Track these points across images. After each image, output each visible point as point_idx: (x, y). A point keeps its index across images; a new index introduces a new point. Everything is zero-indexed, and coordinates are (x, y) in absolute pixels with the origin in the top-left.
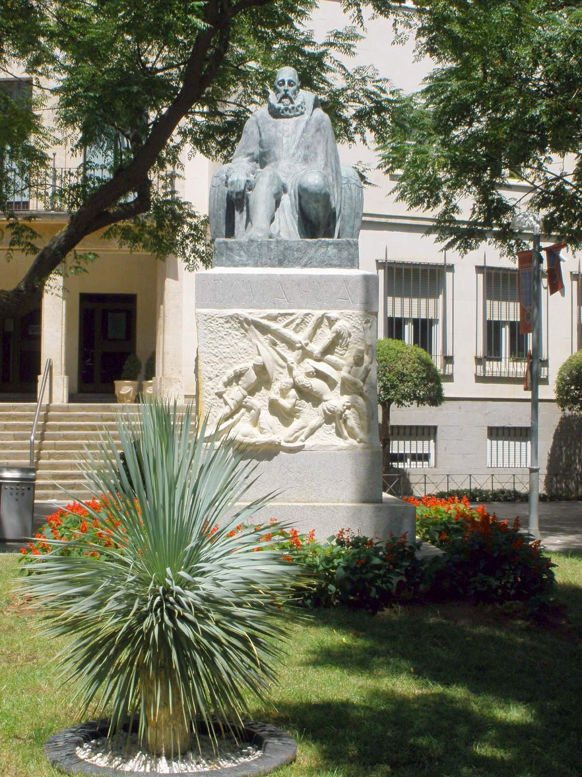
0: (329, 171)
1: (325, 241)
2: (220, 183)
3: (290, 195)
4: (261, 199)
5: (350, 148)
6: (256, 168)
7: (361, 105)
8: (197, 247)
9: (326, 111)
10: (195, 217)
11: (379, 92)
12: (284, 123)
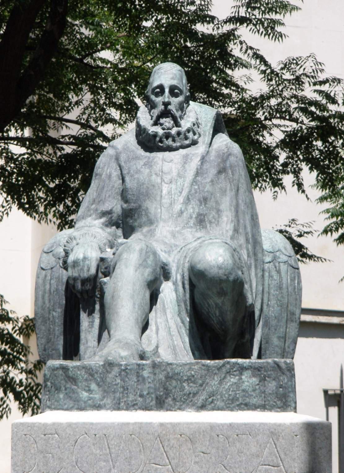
0: (242, 240)
1: (237, 363)
2: (54, 264)
3: (175, 283)
4: (125, 290)
5: (275, 198)
6: (116, 237)
7: (294, 125)
8: (11, 375)
9: (233, 136)
10: (9, 320)
11: (324, 102)
12: (164, 160)
